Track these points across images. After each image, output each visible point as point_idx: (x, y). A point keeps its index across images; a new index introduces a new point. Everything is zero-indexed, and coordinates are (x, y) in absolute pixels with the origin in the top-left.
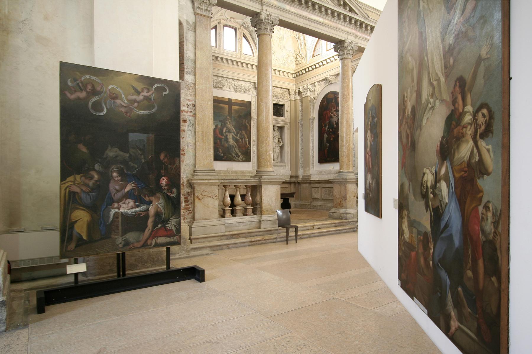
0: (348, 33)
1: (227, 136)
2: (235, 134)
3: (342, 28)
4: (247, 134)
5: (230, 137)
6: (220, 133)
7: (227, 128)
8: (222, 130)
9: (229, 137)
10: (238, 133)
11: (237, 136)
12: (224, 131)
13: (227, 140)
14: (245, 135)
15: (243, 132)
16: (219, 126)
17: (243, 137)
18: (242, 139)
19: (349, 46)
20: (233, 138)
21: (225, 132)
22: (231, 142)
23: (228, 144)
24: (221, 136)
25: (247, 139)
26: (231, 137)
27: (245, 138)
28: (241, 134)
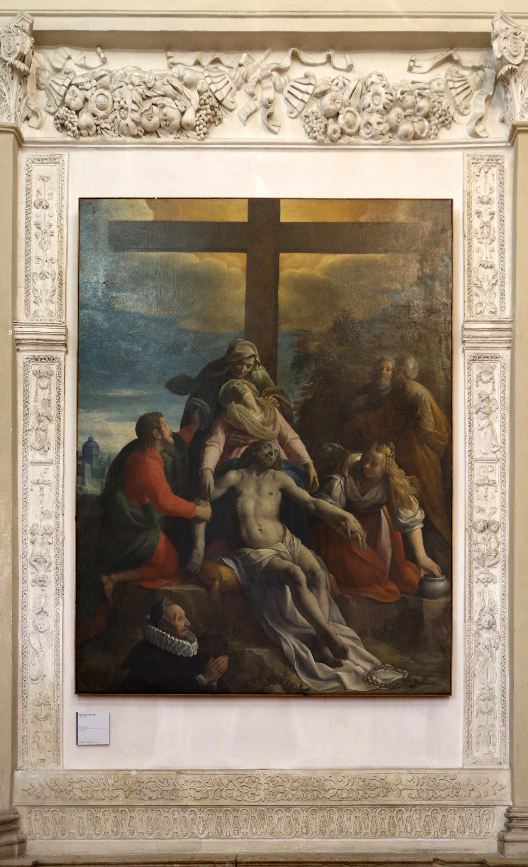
1: (234, 493)
2: (302, 478)
4: (409, 467)
5: (260, 502)
6: (172, 475)
7: (236, 431)
8: (190, 449)
9: (249, 503)
10: (328, 467)
11: (323, 489)
12: (212, 456)
13: (230, 529)
14: (401, 481)
15: (383, 455)
16: (171, 426)
17: (375, 494)
18: (368, 515)
20: (291, 514)
21: (221, 471)
22: (273, 543)
23: (249, 567)
24: (175, 503)
25: (414, 515)
26: (271, 504)
27: (392, 502)
28: (358, 472)
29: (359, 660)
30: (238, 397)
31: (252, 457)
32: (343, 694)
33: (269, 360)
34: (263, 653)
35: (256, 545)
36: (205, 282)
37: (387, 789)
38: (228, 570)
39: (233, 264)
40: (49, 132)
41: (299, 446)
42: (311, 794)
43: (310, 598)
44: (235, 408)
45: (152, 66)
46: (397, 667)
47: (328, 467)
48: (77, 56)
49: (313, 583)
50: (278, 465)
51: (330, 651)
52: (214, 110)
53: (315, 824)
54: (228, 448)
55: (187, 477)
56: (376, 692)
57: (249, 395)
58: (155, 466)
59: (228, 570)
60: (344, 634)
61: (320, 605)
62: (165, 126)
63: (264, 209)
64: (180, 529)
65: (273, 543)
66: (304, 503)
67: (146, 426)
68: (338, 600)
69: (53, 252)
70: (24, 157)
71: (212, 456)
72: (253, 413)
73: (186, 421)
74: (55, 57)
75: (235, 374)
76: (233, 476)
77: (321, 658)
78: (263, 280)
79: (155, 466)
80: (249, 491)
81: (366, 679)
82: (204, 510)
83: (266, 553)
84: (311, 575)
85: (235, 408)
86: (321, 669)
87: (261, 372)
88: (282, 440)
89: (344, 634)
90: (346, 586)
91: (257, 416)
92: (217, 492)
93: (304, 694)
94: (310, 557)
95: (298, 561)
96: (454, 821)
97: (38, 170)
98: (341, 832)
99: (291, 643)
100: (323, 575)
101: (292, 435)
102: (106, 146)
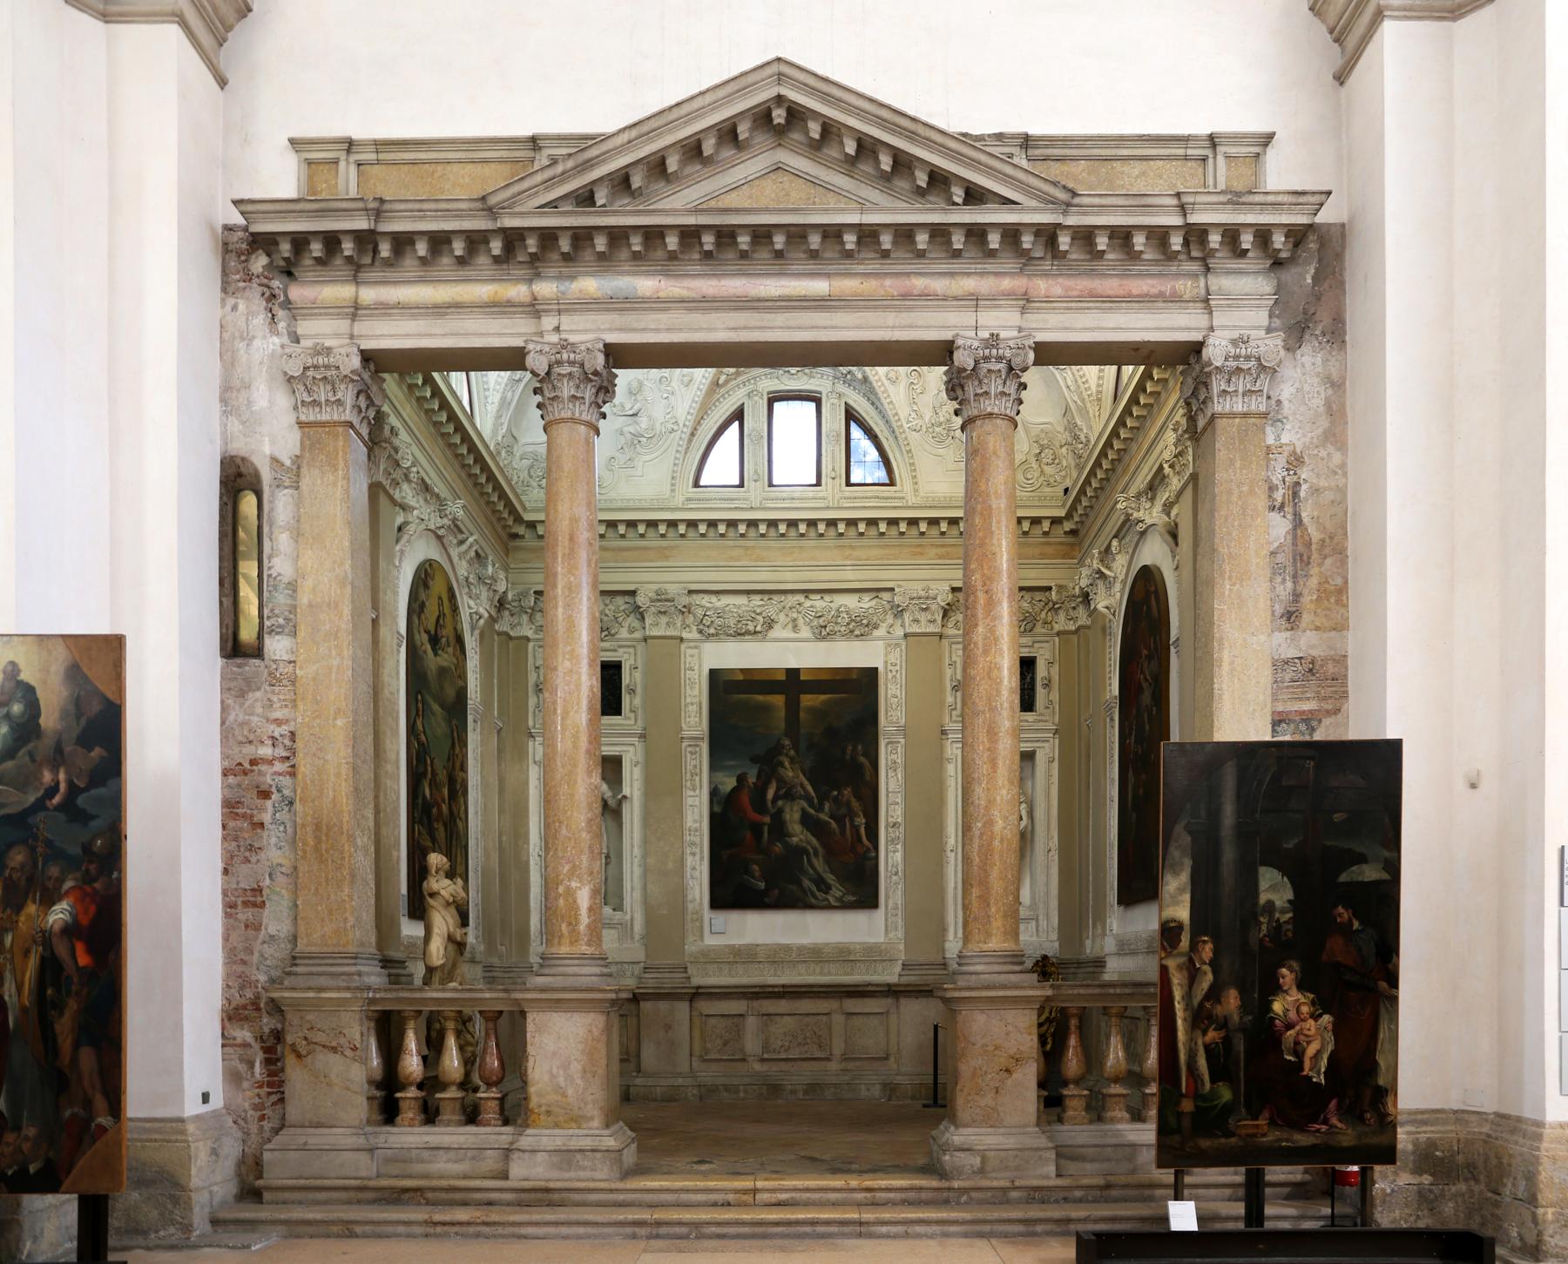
0: (975, 301)
1: (780, 811)
2: (811, 804)
3: (939, 285)
7: (781, 782)
10: (823, 797)
12: (770, 793)
16: (752, 779)
18: (840, 820)
19: (987, 359)
20: (806, 820)
21: (775, 800)
22: (799, 834)
23: (787, 846)
24: (754, 816)
26: (797, 816)
29: (837, 892)
30: (782, 764)
31: (788, 794)
32: (829, 907)
33: (795, 746)
34: (794, 887)
35: (790, 836)
36: (766, 709)
37: (850, 952)
38: (778, 848)
39: (778, 700)
40: (695, 635)
41: (809, 788)
42: (815, 955)
43: (814, 861)
44: (781, 770)
45: (741, 600)
46: (853, 894)
47: (823, 797)
48: (707, 598)
49: (816, 855)
50: (801, 797)
51: (824, 887)
52: (770, 624)
53: (818, 970)
54: (778, 789)
55: (759, 803)
56: (845, 906)
57: (787, 764)
58: (745, 798)
59: (778, 848)
60: (830, 878)
61: (819, 864)
62: (748, 633)
63: (793, 673)
64: (756, 829)
65: (799, 834)
66: (811, 816)
67: (741, 779)
68: (827, 862)
69: (696, 692)
70: (683, 646)
71: (770, 793)
72: (789, 772)
73: (759, 777)
74: (697, 599)
75: (780, 754)
76: (780, 803)
77: (819, 890)
78: (793, 707)
79: (745, 798)
80: (787, 809)
81: (839, 900)
82: (767, 819)
83: (795, 839)
84: (815, 849)
85: (781, 770)
86: (820, 895)
87: (792, 753)
88: (802, 785)
89: (830, 878)
90: (831, 853)
91: (791, 774)
92: (773, 811)
93: (811, 907)
94: (815, 842)
95: (809, 843)
96: (880, 967)
97: (689, 651)
98: (830, 973)
99: (806, 883)
100: (820, 850)
101: (806, 783)
102: (720, 640)
